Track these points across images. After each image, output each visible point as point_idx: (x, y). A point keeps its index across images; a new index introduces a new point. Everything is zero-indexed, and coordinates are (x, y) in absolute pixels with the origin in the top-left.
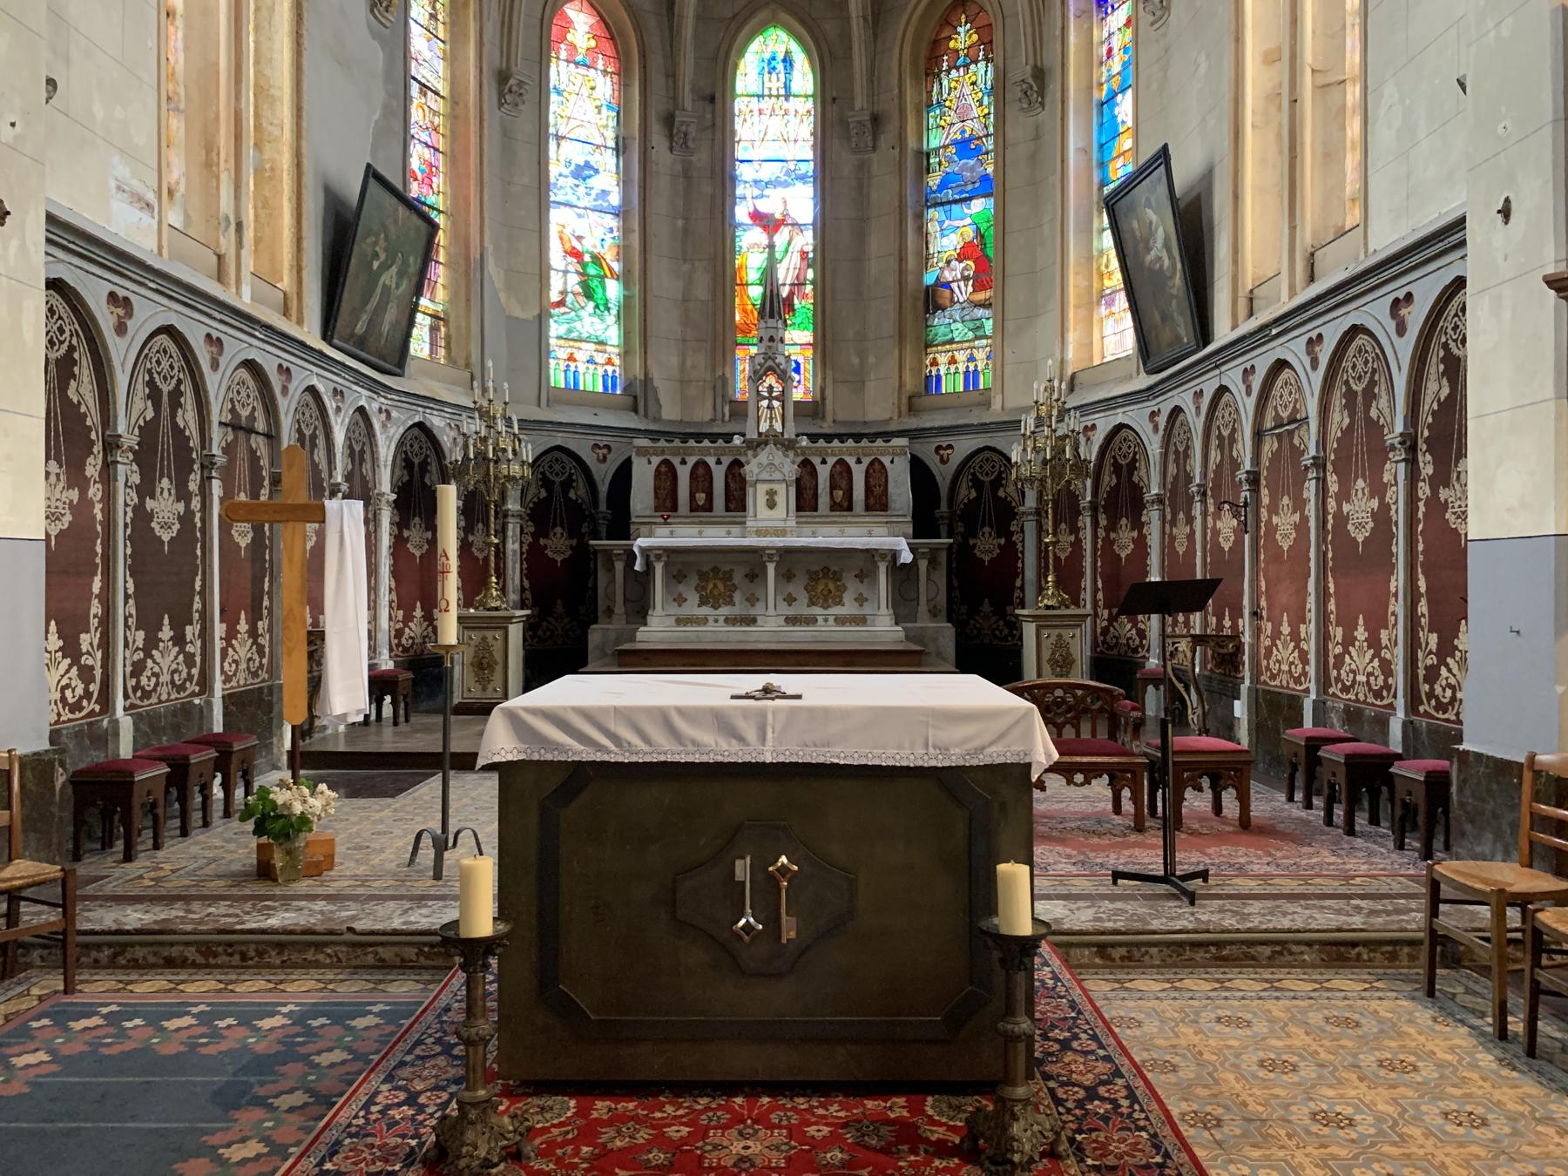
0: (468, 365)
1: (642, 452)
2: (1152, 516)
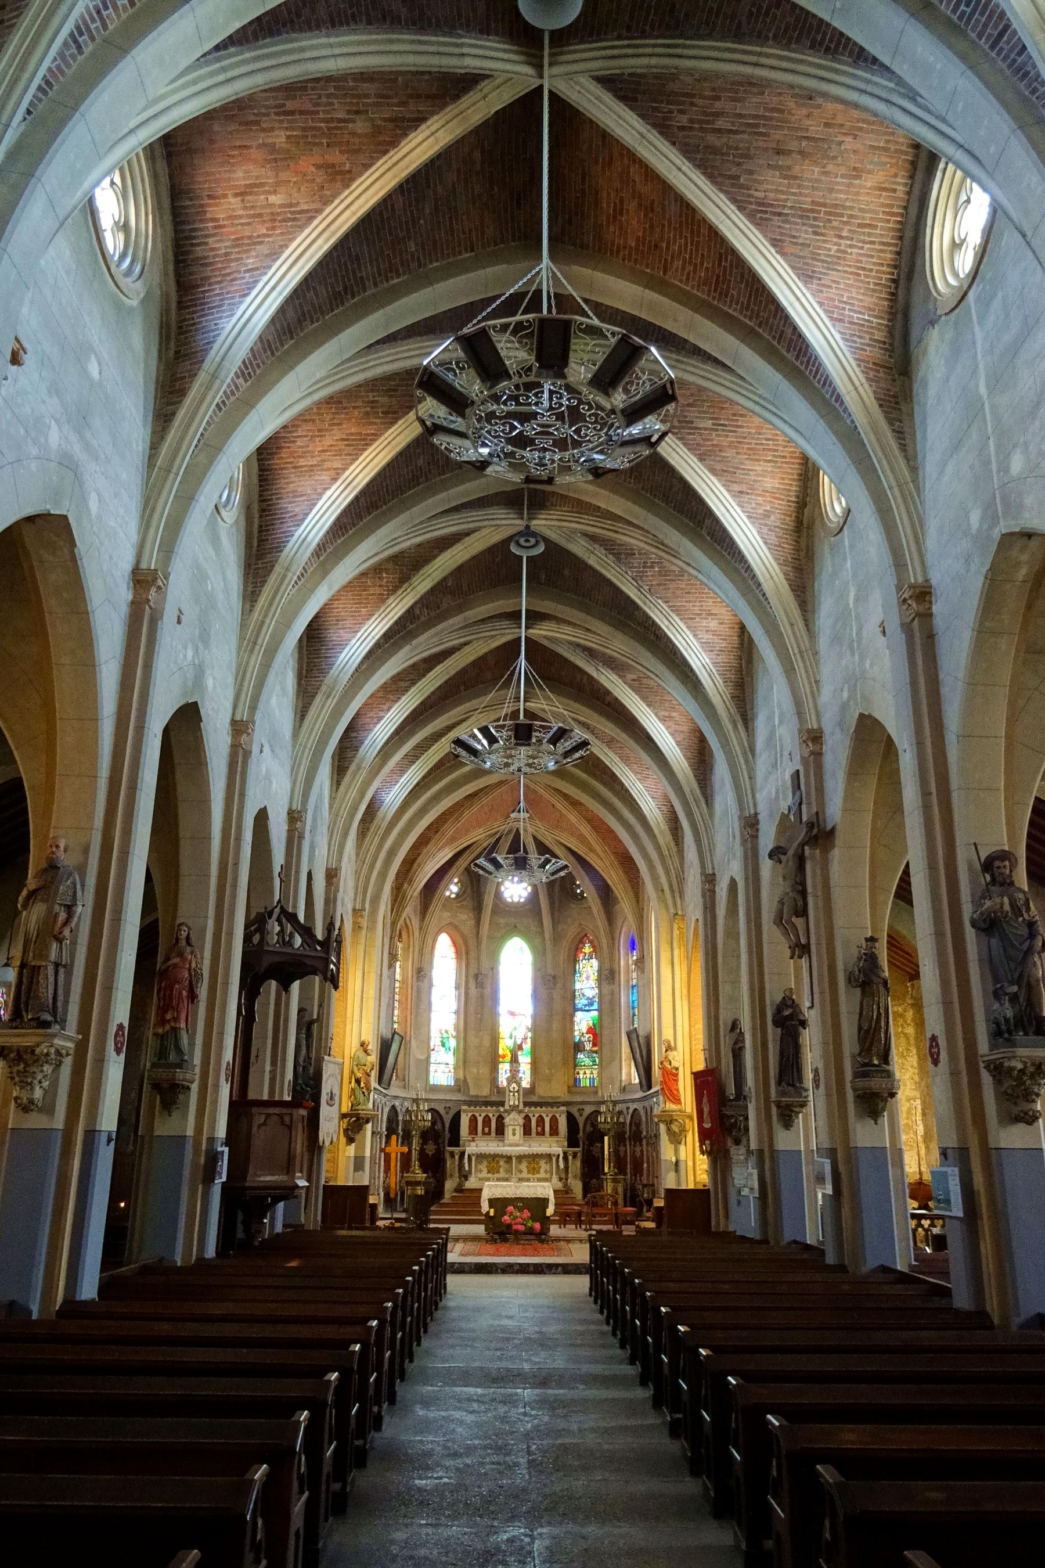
0: (404, 1080)
1: (465, 1111)
2: (644, 1142)
